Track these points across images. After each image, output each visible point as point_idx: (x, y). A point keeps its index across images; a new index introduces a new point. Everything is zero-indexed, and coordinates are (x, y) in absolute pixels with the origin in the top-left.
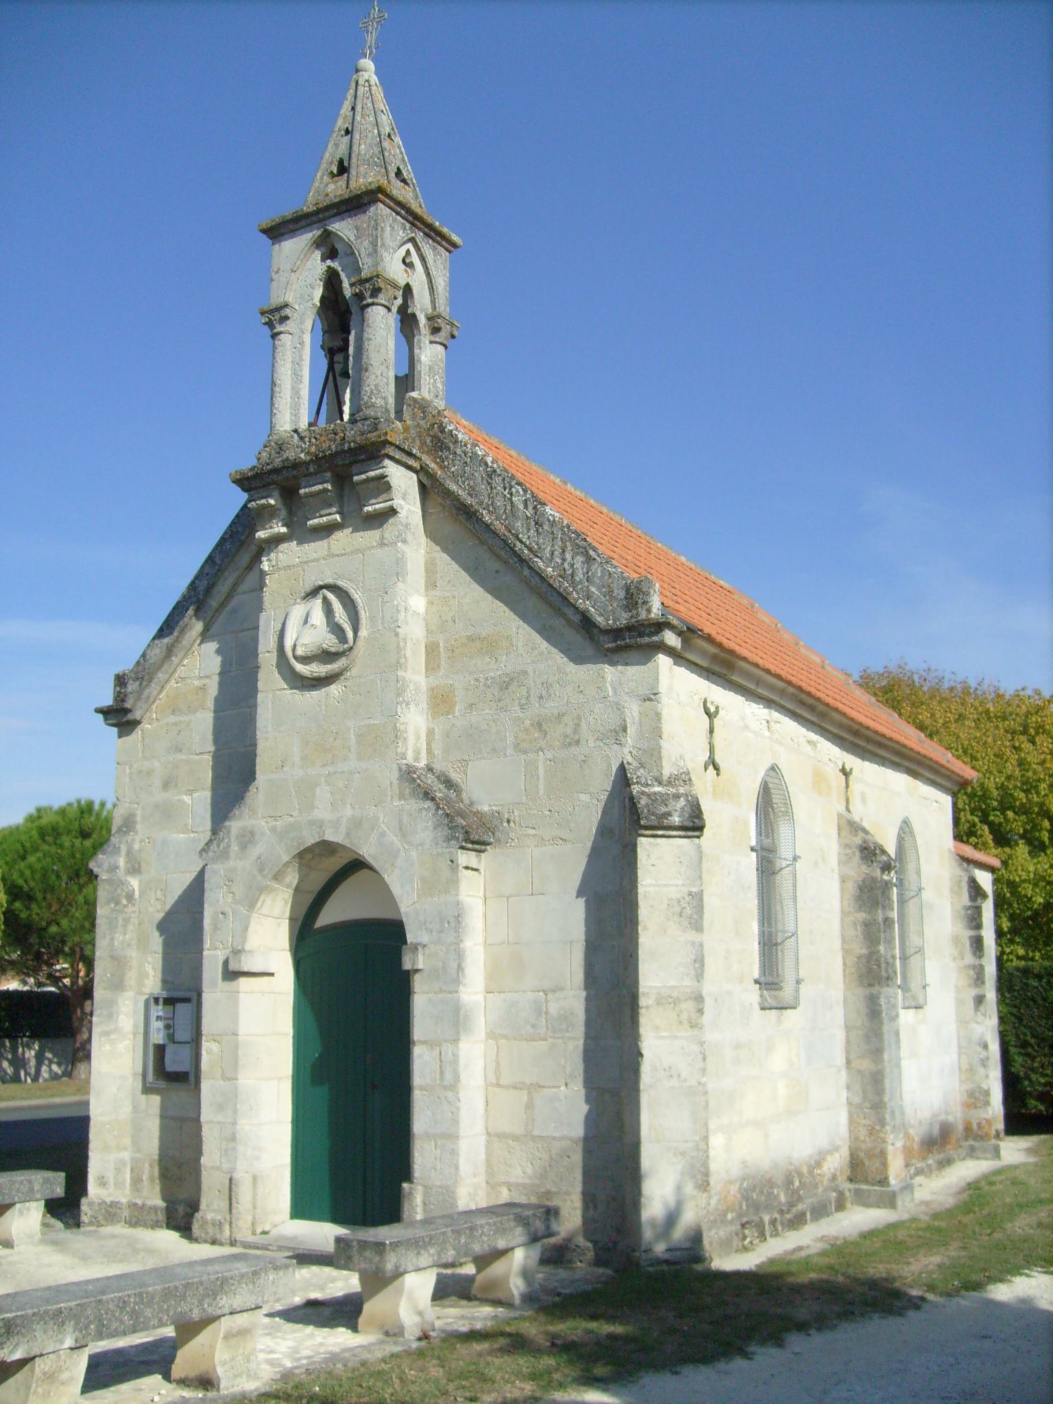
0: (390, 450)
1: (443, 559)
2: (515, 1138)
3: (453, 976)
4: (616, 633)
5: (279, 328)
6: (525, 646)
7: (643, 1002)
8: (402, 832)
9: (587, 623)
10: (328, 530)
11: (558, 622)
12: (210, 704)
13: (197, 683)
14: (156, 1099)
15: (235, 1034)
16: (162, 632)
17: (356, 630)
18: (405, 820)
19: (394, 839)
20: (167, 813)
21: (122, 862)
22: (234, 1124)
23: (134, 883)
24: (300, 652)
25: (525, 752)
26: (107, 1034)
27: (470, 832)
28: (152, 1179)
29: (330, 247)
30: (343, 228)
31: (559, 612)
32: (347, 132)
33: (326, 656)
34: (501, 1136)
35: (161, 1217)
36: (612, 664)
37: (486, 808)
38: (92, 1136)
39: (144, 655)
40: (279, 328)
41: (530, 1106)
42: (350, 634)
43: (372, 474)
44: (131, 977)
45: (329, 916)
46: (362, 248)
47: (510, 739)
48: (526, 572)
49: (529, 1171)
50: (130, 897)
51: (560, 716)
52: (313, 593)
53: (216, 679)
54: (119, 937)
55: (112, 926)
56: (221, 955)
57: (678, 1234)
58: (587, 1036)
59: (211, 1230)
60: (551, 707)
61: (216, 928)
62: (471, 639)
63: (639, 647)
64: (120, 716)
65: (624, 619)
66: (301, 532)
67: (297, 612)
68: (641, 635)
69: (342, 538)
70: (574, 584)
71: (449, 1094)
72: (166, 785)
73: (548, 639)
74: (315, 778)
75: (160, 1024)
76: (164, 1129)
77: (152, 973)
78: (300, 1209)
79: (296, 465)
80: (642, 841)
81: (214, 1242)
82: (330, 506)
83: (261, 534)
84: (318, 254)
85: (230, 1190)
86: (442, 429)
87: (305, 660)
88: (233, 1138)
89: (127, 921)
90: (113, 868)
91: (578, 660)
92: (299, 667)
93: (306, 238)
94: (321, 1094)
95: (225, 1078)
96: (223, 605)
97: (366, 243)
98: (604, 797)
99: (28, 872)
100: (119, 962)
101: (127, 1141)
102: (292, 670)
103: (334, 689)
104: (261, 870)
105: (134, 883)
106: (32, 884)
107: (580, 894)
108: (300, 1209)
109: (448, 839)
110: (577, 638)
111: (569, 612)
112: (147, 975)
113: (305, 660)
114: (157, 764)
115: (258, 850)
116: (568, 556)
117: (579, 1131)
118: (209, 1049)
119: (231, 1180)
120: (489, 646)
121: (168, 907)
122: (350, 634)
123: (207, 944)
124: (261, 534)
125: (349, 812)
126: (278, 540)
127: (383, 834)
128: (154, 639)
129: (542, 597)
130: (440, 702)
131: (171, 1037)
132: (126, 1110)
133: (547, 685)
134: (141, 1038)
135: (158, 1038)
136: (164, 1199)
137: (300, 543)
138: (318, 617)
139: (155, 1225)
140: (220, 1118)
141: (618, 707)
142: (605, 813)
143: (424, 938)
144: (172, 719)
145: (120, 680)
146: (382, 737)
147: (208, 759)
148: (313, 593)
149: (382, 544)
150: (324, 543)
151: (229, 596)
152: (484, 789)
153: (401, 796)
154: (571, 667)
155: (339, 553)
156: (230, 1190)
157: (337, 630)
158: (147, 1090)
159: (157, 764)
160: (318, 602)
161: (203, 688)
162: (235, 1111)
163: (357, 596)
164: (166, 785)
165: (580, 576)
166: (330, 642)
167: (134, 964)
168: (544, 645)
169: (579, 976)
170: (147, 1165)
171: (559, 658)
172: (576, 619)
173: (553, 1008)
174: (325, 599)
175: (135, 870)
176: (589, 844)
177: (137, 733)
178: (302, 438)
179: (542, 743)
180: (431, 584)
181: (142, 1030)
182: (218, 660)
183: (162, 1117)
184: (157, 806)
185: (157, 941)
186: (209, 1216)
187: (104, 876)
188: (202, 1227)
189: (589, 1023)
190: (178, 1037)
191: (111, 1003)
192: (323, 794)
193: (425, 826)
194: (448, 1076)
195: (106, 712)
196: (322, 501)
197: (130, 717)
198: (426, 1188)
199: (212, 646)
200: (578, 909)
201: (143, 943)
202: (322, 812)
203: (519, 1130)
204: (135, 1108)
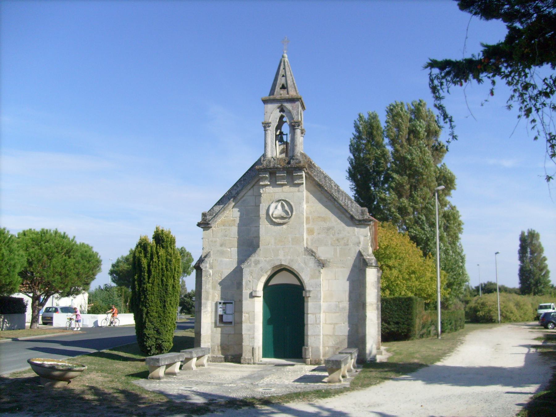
0: (305, 169)
1: (311, 196)
2: (330, 336)
3: (318, 299)
4: (360, 221)
5: (267, 129)
6: (334, 221)
7: (367, 305)
8: (305, 263)
9: (352, 218)
10: (282, 185)
11: (343, 216)
12: (237, 225)
13: (232, 219)
14: (219, 330)
15: (254, 312)
16: (219, 203)
17: (292, 212)
18: (306, 260)
19: (302, 265)
20: (222, 253)
21: (208, 265)
22: (254, 334)
23: (211, 271)
24: (274, 216)
25: (334, 246)
26: (205, 312)
27: (322, 264)
28: (218, 350)
29: (282, 110)
30: (288, 106)
31: (343, 213)
32: (283, 76)
33: (282, 218)
34: (327, 335)
35: (223, 359)
36: (357, 227)
37: (323, 259)
38: (202, 339)
39: (212, 208)
40: (267, 129)
41: (334, 328)
42: (290, 213)
43: (299, 174)
44: (210, 297)
45: (272, 283)
46: (294, 113)
47: (330, 242)
48: (336, 203)
49: (334, 343)
50: (210, 275)
51: (343, 238)
52: (279, 201)
53: (238, 219)
54: (208, 286)
55: (206, 283)
56: (249, 292)
57: (372, 356)
58: (349, 312)
59: (247, 361)
60: (341, 236)
61: (247, 284)
62: (319, 217)
63: (365, 224)
64: (205, 224)
65: (361, 218)
66: (274, 184)
67: (273, 206)
68: (366, 222)
69: (286, 188)
70: (348, 207)
71: (318, 326)
72: (221, 245)
73: (340, 220)
74: (277, 248)
75: (221, 309)
76: (221, 337)
77: (217, 296)
78: (265, 356)
79: (277, 168)
80: (367, 269)
81: (248, 364)
82: (284, 179)
83: (261, 183)
84: (278, 110)
85: (253, 350)
86: (311, 163)
87: (276, 218)
88: (253, 338)
89: (209, 281)
90: (206, 267)
91: (348, 225)
92: (274, 220)
93: (276, 105)
94: (271, 328)
95: (250, 323)
96: (241, 199)
97: (295, 111)
98: (354, 258)
99: (33, 255)
100: (208, 293)
101: (210, 340)
102: (272, 220)
103: (284, 226)
104: (262, 270)
105: (211, 271)
106: (34, 259)
107: (348, 280)
108: (265, 356)
109: (318, 266)
110: (348, 220)
111: (347, 214)
112: (216, 296)
113: (276, 218)
114: (218, 239)
115: (259, 266)
116: (347, 200)
117: (347, 334)
118: (245, 316)
119: (253, 348)
120: (324, 220)
121: (223, 278)
122: (290, 213)
123: (244, 289)
124: (261, 183)
125: (289, 257)
126: (266, 186)
127: (299, 264)
128: (216, 204)
129: (339, 209)
130: (310, 231)
131: (225, 313)
132: (210, 332)
133: (340, 230)
134: (214, 313)
135: (220, 312)
136: (222, 354)
137: (273, 187)
138: (279, 207)
139: (221, 362)
140: (249, 333)
141: (358, 238)
142: (355, 261)
143: (311, 289)
144: (223, 228)
145: (204, 215)
146: (298, 240)
147: (236, 239)
148: (279, 201)
149: (299, 191)
150: (281, 188)
151: (243, 196)
152: (323, 253)
153: (305, 255)
154: (346, 227)
155: (285, 191)
156: (253, 350)
157: (287, 212)
158: (216, 326)
159: (218, 239)
160: (280, 204)
161: (234, 220)
162: (254, 331)
163: (292, 203)
164: (221, 245)
165: (349, 206)
166: (283, 214)
167: (211, 293)
168: (339, 221)
169: (347, 299)
170: (216, 347)
171: (343, 225)
172: (349, 216)
173: (341, 306)
174: (282, 203)
175: (211, 268)
176: (350, 269)
177: (210, 231)
178: (274, 160)
179: (338, 244)
180: (307, 202)
181: (214, 310)
182: (239, 213)
183: (221, 334)
184: (218, 251)
185: (219, 288)
186: (247, 358)
187: (204, 269)
188: (244, 360)
189: (350, 309)
190: (227, 312)
191: (206, 304)
192: (281, 253)
193: (312, 263)
194: (318, 321)
195: (199, 225)
196: (283, 178)
197: (209, 226)
198: (312, 347)
199: (236, 210)
200: (347, 284)
201: (214, 288)
202: (281, 257)
203: (331, 334)
204: (212, 332)
